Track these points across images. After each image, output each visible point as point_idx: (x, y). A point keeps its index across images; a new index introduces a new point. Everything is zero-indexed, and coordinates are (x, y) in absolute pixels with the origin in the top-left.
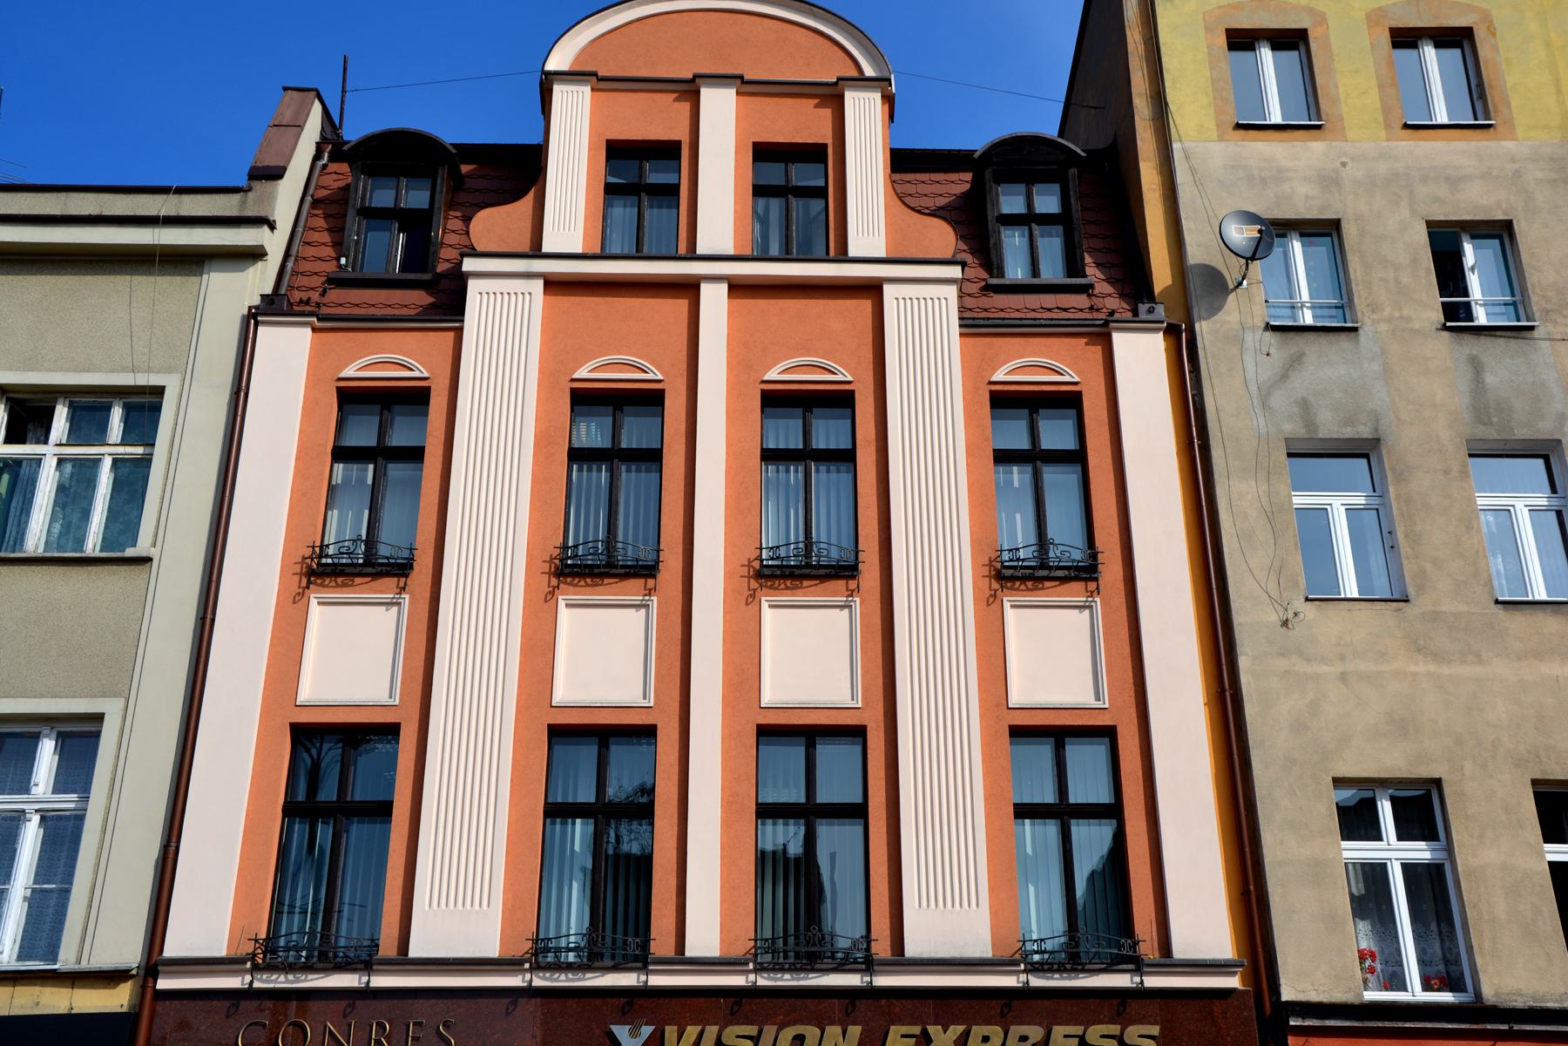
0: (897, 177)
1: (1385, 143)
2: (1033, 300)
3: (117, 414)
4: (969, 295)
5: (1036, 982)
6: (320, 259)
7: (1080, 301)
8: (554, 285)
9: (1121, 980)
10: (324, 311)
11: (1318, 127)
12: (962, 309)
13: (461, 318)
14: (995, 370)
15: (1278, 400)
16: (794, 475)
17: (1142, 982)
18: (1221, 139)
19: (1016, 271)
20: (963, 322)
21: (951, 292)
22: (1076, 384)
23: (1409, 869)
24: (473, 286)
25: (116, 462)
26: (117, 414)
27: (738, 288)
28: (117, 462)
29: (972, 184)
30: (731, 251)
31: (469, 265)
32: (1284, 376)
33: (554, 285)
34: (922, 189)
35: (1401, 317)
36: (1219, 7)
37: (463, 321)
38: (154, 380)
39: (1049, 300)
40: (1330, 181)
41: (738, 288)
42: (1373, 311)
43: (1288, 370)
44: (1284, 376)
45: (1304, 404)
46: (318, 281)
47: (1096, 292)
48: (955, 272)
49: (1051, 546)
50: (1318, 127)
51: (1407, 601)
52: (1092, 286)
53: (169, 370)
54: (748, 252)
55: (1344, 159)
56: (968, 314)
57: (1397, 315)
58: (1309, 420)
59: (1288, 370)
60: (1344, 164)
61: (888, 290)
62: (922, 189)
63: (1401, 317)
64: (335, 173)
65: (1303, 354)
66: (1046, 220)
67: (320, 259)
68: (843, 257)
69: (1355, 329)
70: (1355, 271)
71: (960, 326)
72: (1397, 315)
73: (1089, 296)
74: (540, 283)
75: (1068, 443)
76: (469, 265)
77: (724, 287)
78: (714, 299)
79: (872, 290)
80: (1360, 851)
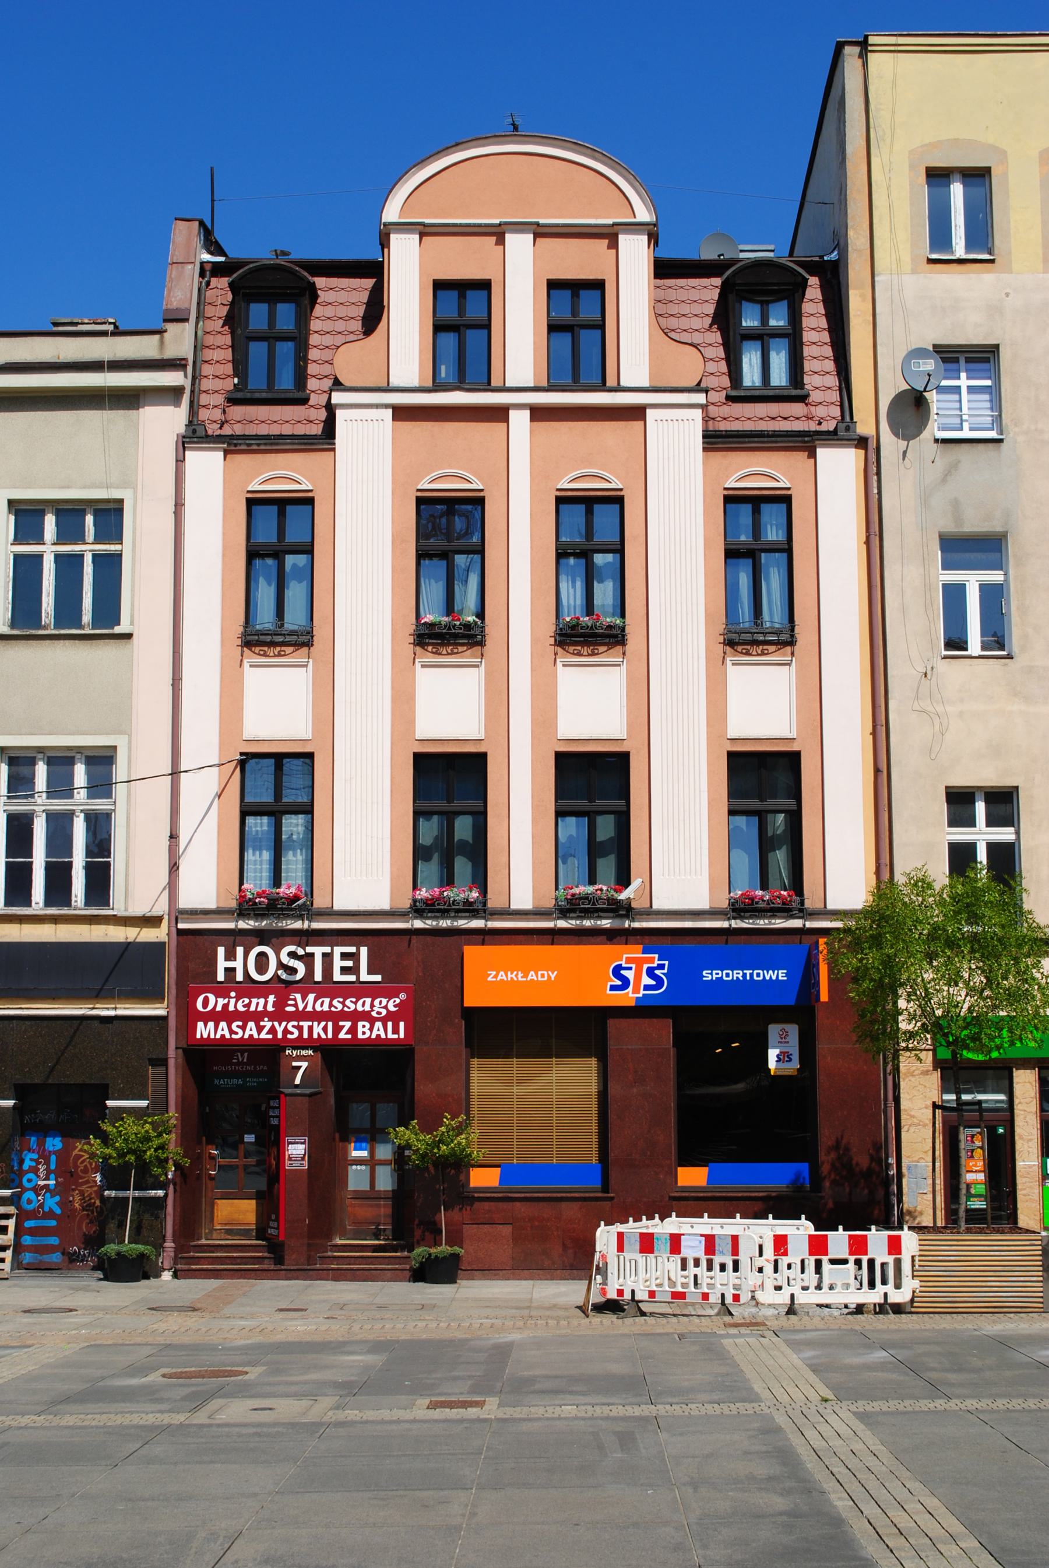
0: (660, 282)
1: (1041, 275)
3: (89, 519)
4: (713, 404)
7: (797, 409)
8: (401, 413)
9: (796, 923)
11: (992, 261)
12: (707, 419)
13: (332, 441)
14: (728, 477)
18: (914, 272)
19: (751, 375)
20: (706, 446)
21: (698, 413)
23: (992, 847)
24: (340, 414)
25: (95, 556)
26: (89, 519)
27: (539, 413)
28: (96, 557)
29: (721, 290)
32: (944, 480)
33: (401, 413)
34: (682, 295)
35: (1036, 430)
36: (922, 146)
38: (116, 494)
39: (773, 408)
40: (995, 310)
41: (539, 413)
42: (1016, 425)
43: (946, 475)
44: (944, 480)
45: (956, 504)
46: (219, 399)
47: (810, 399)
50: (992, 261)
51: (1012, 658)
52: (807, 396)
53: (124, 485)
54: (545, 384)
55: (1008, 291)
57: (1033, 427)
58: (958, 519)
59: (946, 475)
60: (1007, 295)
61: (649, 412)
62: (682, 295)
63: (1036, 430)
65: (959, 462)
66: (777, 334)
69: (1000, 441)
70: (1006, 390)
71: (703, 443)
72: (1033, 427)
76: (337, 398)
77: (527, 413)
78: (519, 420)
79: (638, 413)
80: (961, 835)
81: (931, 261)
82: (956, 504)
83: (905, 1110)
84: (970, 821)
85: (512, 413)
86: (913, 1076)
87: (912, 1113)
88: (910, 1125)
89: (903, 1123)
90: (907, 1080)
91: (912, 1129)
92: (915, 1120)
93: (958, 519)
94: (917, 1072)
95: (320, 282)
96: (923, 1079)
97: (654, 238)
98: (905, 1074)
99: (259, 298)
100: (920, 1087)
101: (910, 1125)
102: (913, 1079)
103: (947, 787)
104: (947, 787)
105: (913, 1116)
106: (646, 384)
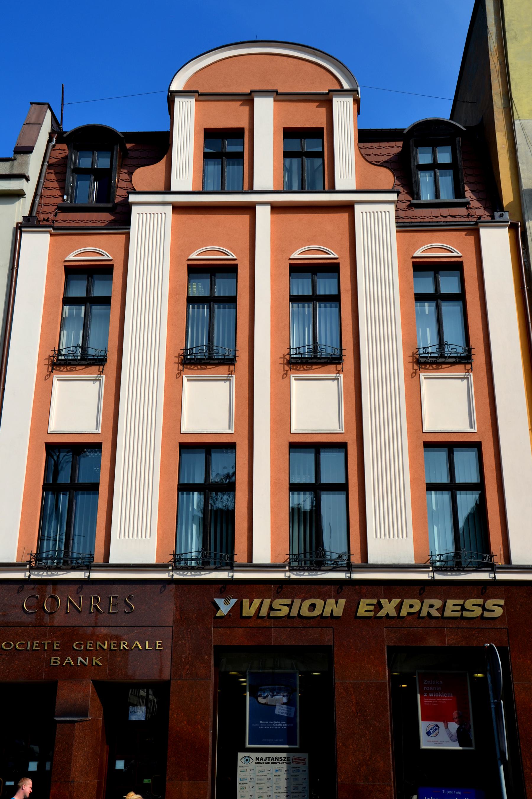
2: (436, 212)
4: (401, 209)
5: (438, 576)
6: (53, 196)
7: (462, 211)
8: (178, 208)
10: (56, 224)
12: (397, 218)
13: (128, 227)
14: (415, 250)
17: (495, 577)
19: (427, 196)
20: (398, 224)
21: (392, 208)
22: (460, 257)
24: (135, 210)
29: (403, 148)
30: (272, 188)
31: (132, 198)
33: (178, 208)
34: (375, 151)
37: (130, 229)
39: (445, 211)
46: (52, 209)
47: (471, 206)
48: (394, 197)
49: (446, 346)
52: (468, 203)
54: (281, 188)
56: (401, 220)
61: (357, 207)
62: (375, 151)
64: (60, 149)
66: (444, 167)
67: (53, 196)
68: (332, 190)
71: (397, 227)
73: (467, 208)
74: (170, 207)
75: (455, 289)
76: (132, 198)
77: (268, 208)
85: (258, 209)
106: (354, 188)
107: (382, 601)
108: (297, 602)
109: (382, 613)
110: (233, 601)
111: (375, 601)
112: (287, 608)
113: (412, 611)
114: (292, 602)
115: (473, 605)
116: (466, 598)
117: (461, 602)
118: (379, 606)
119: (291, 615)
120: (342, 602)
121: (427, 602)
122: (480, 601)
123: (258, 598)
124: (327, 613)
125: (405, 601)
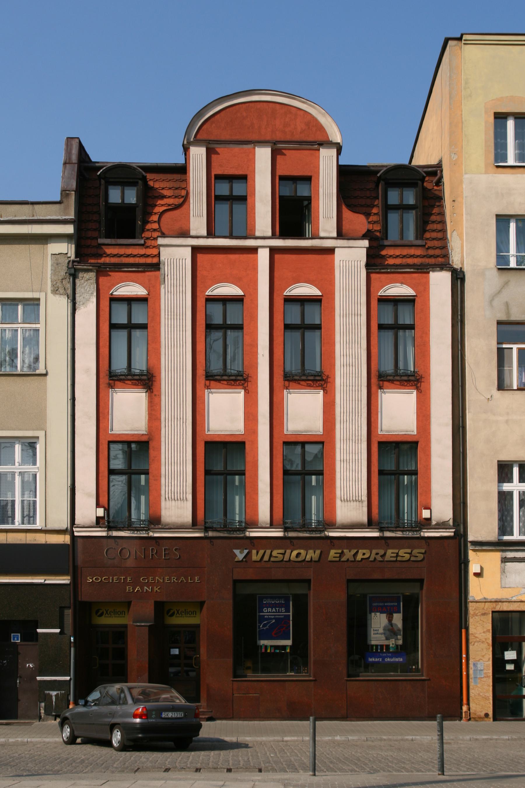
15: (496, 303)
16: (297, 335)
18: (486, 173)
43: (502, 288)
45: (507, 305)
58: (508, 313)
59: (502, 288)
68: (316, 237)
81: (498, 167)
82: (507, 305)
83: (472, 634)
84: (510, 480)
86: (477, 616)
87: (476, 635)
88: (475, 642)
89: (470, 641)
90: (474, 618)
91: (476, 644)
92: (478, 639)
93: (508, 313)
94: (479, 614)
95: (149, 176)
96: (482, 618)
97: (339, 153)
98: (473, 615)
99: (115, 184)
100: (481, 622)
101: (475, 642)
102: (477, 617)
103: (498, 461)
104: (498, 461)
105: (477, 637)
107: (345, 551)
108: (288, 551)
109: (344, 559)
110: (246, 551)
111: (340, 551)
112: (281, 556)
113: (365, 557)
114: (285, 552)
115: (405, 553)
116: (400, 549)
117: (396, 551)
118: (342, 554)
119: (285, 560)
120: (318, 552)
121: (374, 551)
122: (409, 551)
123: (262, 549)
124: (308, 558)
125: (360, 551)
